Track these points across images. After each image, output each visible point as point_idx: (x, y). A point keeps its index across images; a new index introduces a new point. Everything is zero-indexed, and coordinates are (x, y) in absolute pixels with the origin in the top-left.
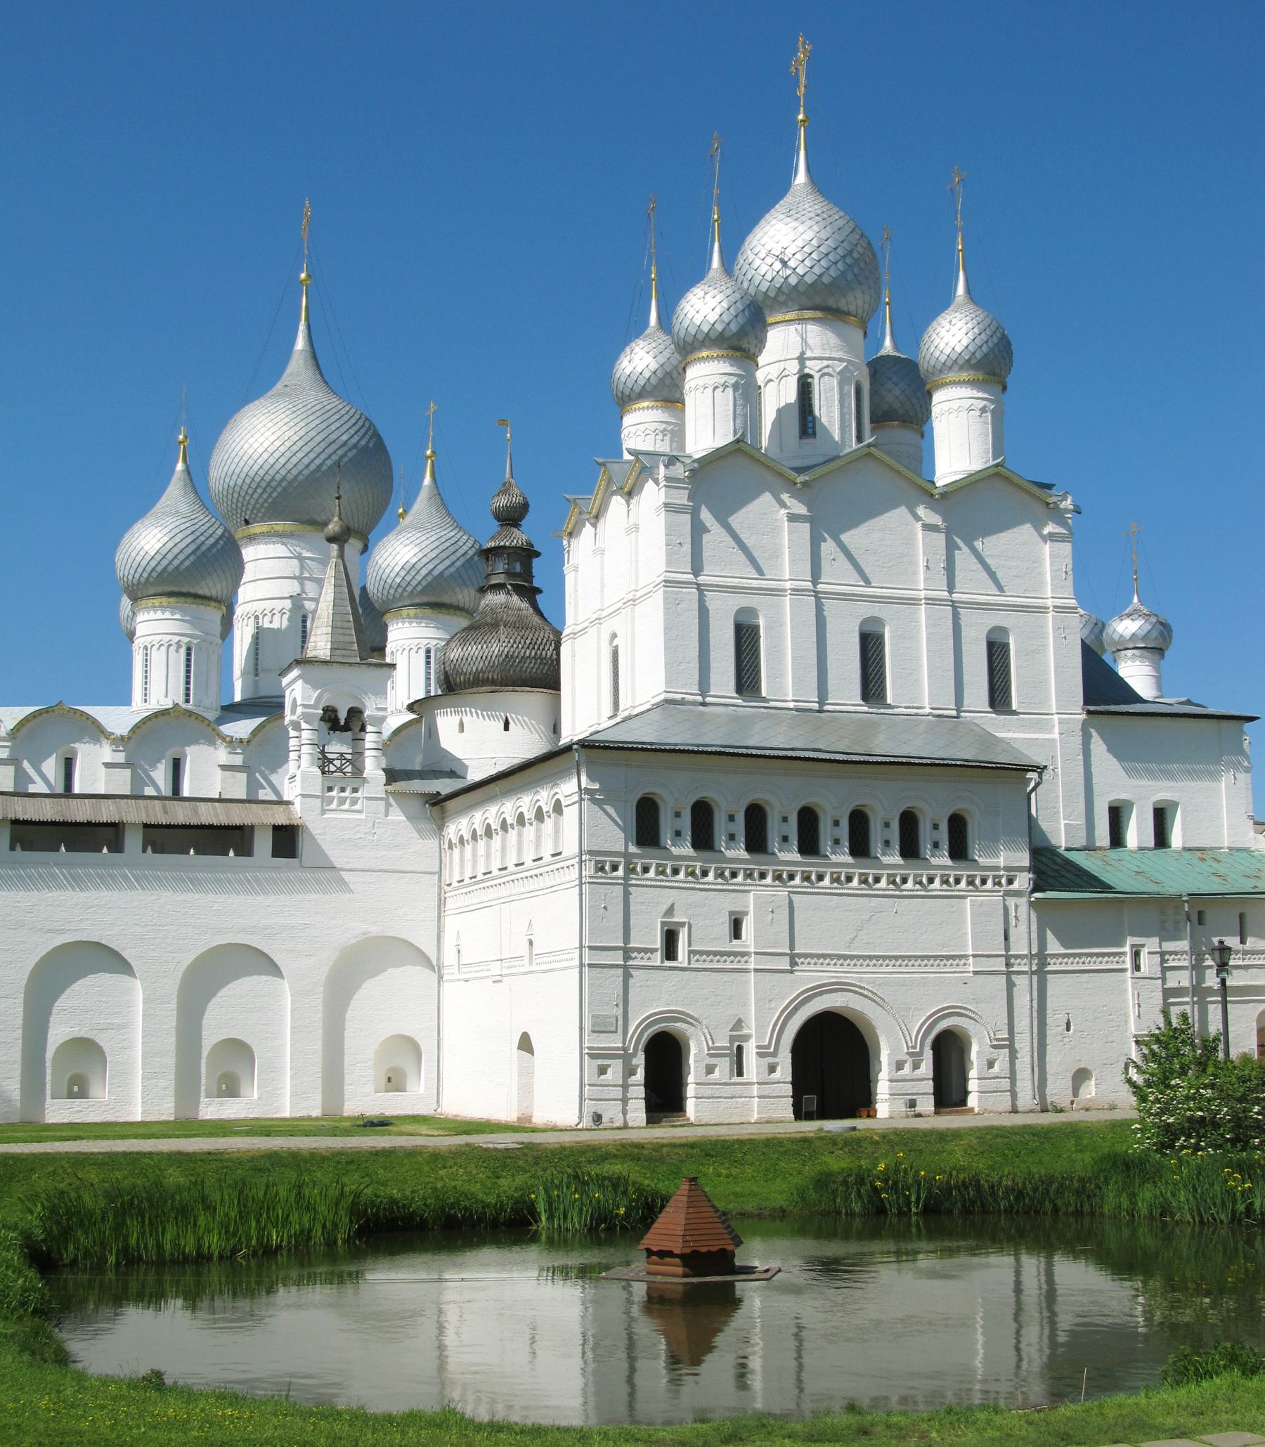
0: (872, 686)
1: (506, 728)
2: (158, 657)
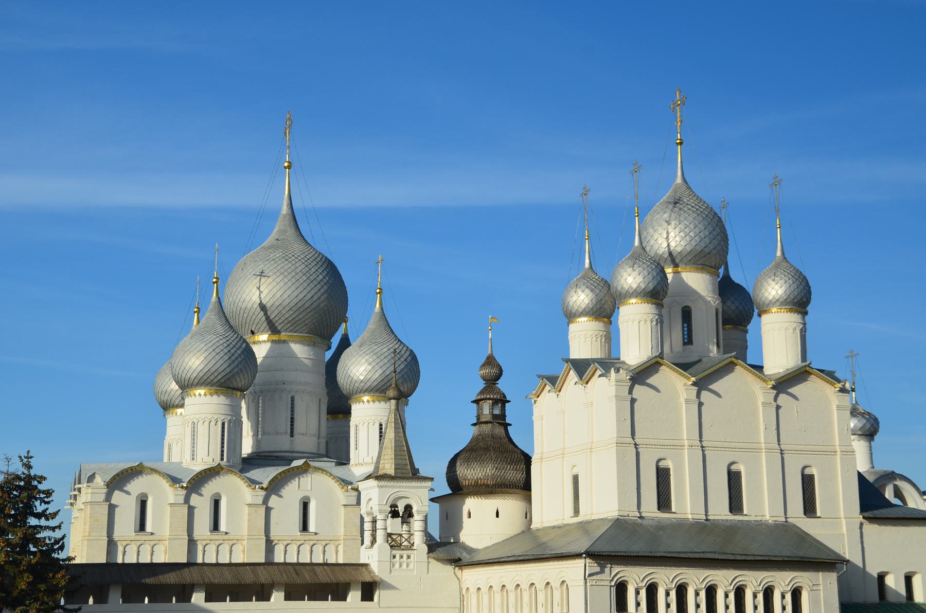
0: (735, 504)
1: (497, 516)
2: (202, 430)
